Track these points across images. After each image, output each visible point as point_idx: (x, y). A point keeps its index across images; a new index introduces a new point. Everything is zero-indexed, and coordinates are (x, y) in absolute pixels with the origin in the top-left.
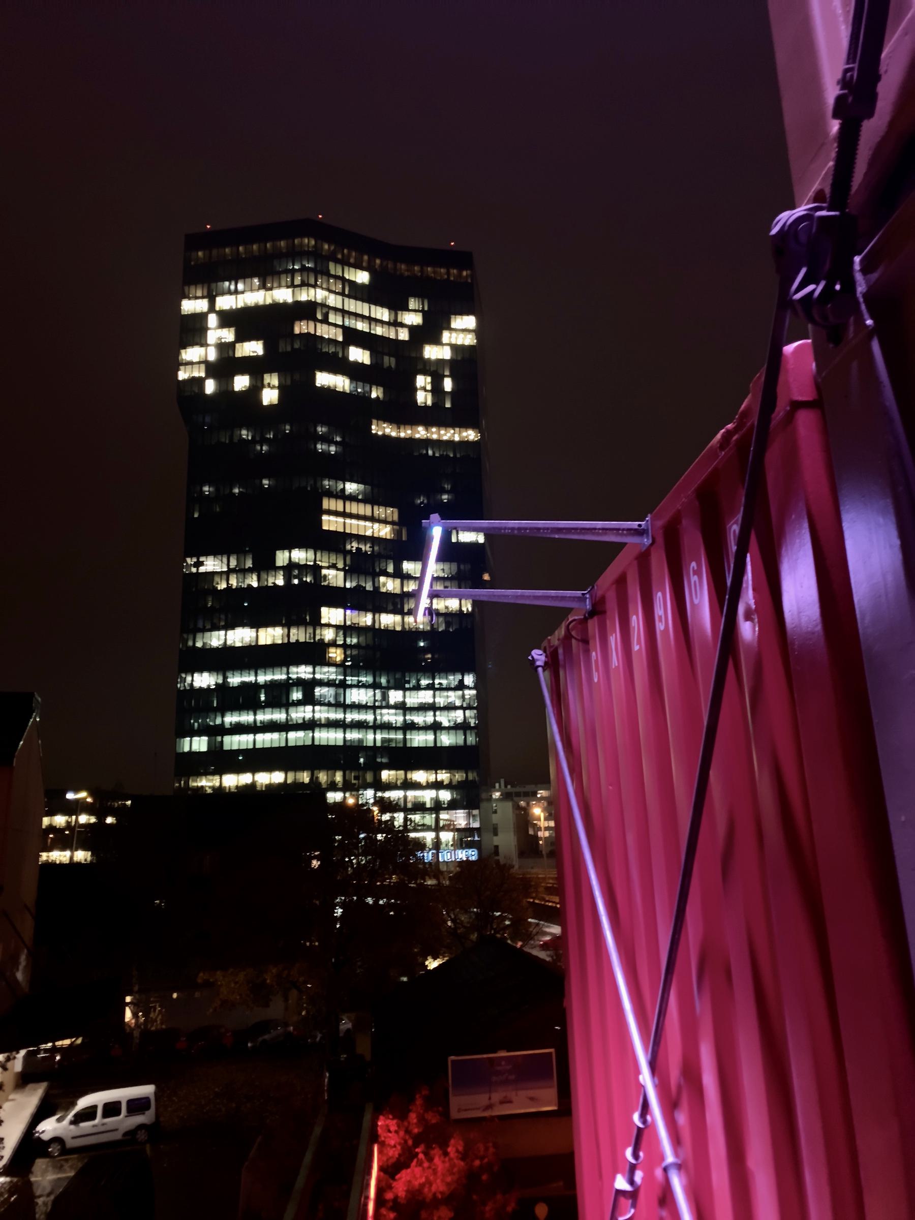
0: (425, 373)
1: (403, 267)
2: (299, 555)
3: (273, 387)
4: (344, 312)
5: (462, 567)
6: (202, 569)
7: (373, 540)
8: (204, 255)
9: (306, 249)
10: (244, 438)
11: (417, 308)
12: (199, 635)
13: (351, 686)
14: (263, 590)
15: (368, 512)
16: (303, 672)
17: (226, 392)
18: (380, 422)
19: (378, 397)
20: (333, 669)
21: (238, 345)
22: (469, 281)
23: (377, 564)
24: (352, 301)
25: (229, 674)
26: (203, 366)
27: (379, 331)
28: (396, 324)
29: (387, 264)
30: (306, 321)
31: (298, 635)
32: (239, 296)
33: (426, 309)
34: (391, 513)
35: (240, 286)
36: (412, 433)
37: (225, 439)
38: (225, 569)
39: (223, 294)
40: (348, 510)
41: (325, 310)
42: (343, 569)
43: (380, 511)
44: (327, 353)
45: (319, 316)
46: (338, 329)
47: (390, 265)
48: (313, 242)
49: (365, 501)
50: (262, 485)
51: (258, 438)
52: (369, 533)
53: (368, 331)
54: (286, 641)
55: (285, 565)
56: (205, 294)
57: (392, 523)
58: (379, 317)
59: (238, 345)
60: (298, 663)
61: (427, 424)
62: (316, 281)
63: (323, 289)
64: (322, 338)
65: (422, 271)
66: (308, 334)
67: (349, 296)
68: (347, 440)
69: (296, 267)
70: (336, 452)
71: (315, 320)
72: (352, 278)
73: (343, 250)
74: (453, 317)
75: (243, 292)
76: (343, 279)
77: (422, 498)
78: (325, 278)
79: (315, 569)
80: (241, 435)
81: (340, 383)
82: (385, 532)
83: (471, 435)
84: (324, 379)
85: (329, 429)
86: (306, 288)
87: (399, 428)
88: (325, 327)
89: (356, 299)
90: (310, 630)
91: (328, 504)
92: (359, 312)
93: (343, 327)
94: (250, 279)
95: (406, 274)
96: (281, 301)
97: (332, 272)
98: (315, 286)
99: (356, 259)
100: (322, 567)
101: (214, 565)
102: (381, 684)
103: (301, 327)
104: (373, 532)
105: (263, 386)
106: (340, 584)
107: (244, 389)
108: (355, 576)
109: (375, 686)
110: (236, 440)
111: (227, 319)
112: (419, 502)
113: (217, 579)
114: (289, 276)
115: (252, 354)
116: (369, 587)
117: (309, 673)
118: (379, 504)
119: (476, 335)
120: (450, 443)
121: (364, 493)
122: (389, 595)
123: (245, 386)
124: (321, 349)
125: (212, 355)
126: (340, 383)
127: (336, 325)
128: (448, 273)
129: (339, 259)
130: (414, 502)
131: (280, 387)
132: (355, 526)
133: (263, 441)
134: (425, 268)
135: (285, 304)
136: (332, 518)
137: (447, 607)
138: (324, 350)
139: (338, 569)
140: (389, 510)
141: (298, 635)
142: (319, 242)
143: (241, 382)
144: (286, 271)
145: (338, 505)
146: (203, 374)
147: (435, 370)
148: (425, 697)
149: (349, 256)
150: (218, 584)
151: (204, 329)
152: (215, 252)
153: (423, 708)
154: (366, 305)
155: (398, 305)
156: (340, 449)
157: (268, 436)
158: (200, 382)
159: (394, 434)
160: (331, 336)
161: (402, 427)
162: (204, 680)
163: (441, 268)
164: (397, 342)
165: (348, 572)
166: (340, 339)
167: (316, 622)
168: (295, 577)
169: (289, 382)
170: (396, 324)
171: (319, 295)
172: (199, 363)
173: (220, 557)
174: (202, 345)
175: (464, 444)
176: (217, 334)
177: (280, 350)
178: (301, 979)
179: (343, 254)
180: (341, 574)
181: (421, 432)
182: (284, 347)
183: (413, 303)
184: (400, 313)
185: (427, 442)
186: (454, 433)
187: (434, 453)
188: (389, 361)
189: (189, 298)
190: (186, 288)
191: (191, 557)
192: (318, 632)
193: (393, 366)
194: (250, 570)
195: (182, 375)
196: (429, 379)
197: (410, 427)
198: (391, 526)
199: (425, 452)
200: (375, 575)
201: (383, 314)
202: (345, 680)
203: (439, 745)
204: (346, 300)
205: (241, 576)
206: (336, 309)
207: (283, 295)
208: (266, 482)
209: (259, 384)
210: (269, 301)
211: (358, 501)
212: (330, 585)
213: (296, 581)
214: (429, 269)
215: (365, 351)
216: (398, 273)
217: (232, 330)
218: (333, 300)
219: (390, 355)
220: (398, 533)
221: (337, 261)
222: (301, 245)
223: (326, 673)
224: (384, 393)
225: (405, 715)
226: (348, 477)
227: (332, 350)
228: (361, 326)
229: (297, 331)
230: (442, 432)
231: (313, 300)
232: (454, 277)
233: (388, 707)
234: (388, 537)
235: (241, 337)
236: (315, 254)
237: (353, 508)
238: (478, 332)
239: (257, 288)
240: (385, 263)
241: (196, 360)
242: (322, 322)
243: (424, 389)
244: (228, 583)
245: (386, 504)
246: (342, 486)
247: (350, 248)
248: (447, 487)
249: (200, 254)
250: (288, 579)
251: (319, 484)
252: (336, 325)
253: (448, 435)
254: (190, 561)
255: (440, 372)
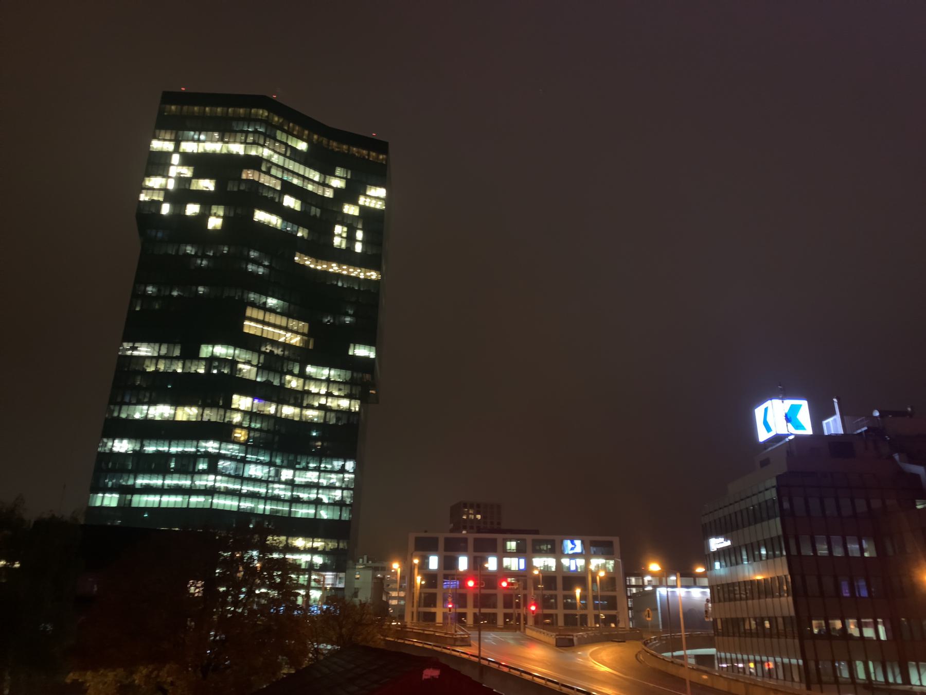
0: (342, 224)
1: (335, 144)
2: (220, 351)
3: (218, 217)
4: (284, 169)
5: (355, 375)
6: (136, 353)
7: (286, 346)
8: (176, 108)
9: (260, 118)
10: (188, 253)
11: (342, 176)
12: (124, 408)
13: (250, 462)
14: (186, 375)
15: (284, 324)
16: (211, 446)
17: (178, 216)
18: (302, 255)
19: (303, 236)
20: (236, 447)
21: (194, 181)
22: (384, 162)
23: (285, 365)
24: (292, 162)
25: (146, 442)
26: (162, 193)
27: (310, 187)
28: (324, 185)
29: (323, 139)
30: (252, 171)
31: (211, 415)
32: (201, 145)
33: (349, 177)
34: (303, 326)
35: (202, 137)
36: (327, 267)
37: (171, 251)
38: (156, 354)
39: (187, 140)
40: (267, 320)
41: (269, 165)
42: (257, 366)
43: (293, 324)
44: (266, 197)
45: (264, 169)
46: (278, 181)
47: (325, 141)
48: (266, 114)
49: (282, 314)
50: (197, 291)
51: (200, 254)
52: (282, 340)
53: (301, 186)
54: (199, 419)
55: (208, 357)
56: (173, 138)
57: (303, 334)
58: (311, 177)
59: (194, 181)
60: (207, 439)
61: (340, 262)
62: (265, 142)
63: (269, 149)
64: (263, 185)
65: (349, 150)
66: (253, 180)
67: (290, 158)
68: (273, 265)
69: (250, 130)
70: (263, 273)
71: (260, 170)
72: (294, 145)
73: (289, 124)
74: (368, 186)
75: (204, 142)
76: (286, 145)
77: (329, 318)
78: (272, 141)
79: (233, 363)
80: (185, 250)
81: (274, 221)
82: (296, 340)
83: (373, 275)
84: (260, 216)
85: (260, 254)
86: (256, 146)
87: (317, 262)
88: (267, 177)
89: (295, 160)
90: (222, 412)
91: (250, 312)
92: (296, 171)
93: (281, 179)
94: (211, 133)
95: (337, 149)
96: (235, 153)
97: (279, 138)
98: (263, 146)
99: (298, 132)
100: (238, 362)
101: (147, 352)
102: (276, 463)
103: (248, 174)
104: (285, 340)
105: (210, 215)
106: (252, 377)
107: (194, 215)
108: (265, 373)
109: (270, 464)
110: (181, 253)
111: (187, 159)
112: (326, 320)
113: (147, 362)
114: (244, 135)
115: (205, 189)
116: (276, 382)
117: (216, 448)
118: (294, 318)
119: (386, 203)
120: (357, 278)
121: (282, 308)
122: (292, 391)
123: (195, 213)
124: (262, 193)
125: (171, 185)
126: (274, 221)
127: (276, 178)
128: (369, 155)
129: (284, 129)
130: (322, 321)
131: (225, 218)
132: (270, 332)
133: (204, 256)
134: (351, 148)
135: (238, 155)
136: (253, 324)
137: (339, 406)
138: (264, 195)
139: (252, 365)
140: (301, 324)
141: (211, 415)
142: (271, 114)
143: (192, 209)
144: (242, 131)
145: (259, 315)
146: (161, 199)
147: (350, 223)
148: (312, 477)
149: (294, 129)
150: (147, 366)
151: (168, 164)
152: (185, 108)
153: (309, 486)
154: (302, 167)
155: (327, 171)
156: (267, 271)
157: (208, 254)
158: (158, 204)
159: (312, 266)
160: (271, 185)
161: (320, 261)
162: (122, 446)
163: (364, 149)
164: (323, 197)
165: (260, 368)
166: (279, 188)
167: (227, 406)
168: (215, 367)
169: (232, 214)
170: (324, 185)
171: (266, 153)
172: (160, 190)
173: (152, 344)
174: (164, 176)
175: (367, 281)
176: (177, 169)
177: (228, 189)
178: (170, 679)
179: (289, 127)
180: (255, 369)
181: (334, 268)
182: (232, 187)
183: (339, 171)
184: (328, 177)
185: (338, 276)
186: (361, 272)
187: (343, 285)
188: (315, 211)
189: (159, 140)
190: (157, 131)
191: (128, 341)
192: (228, 414)
193: (318, 215)
194: (177, 358)
195: (143, 197)
196: (345, 229)
197: (326, 262)
198: (302, 336)
199: (335, 283)
200: (283, 373)
201: (316, 176)
202: (245, 457)
203: (318, 517)
204: (287, 160)
205: (168, 362)
206: (277, 166)
207: (237, 148)
208: (201, 290)
209: (207, 213)
210: (224, 151)
211: (277, 313)
212: (244, 377)
213: (215, 371)
214: (355, 149)
215: (297, 201)
216: (330, 148)
217: (191, 168)
218: (276, 158)
219: (316, 206)
220: (306, 343)
221: (283, 131)
222: (257, 114)
223: (231, 449)
224: (309, 234)
225: (292, 491)
226: (270, 293)
227: (270, 195)
228: (295, 181)
229: (244, 176)
230: (351, 270)
231: (261, 156)
232: (373, 158)
233: (280, 482)
234: (298, 345)
235: (198, 175)
236: (266, 122)
237: (271, 318)
238: (387, 200)
239: (217, 140)
240: (321, 139)
241: (157, 187)
242: (265, 173)
243: (340, 235)
244: (156, 368)
245: (299, 318)
246: (264, 300)
247: (294, 123)
248: (351, 312)
249: (173, 108)
250: (208, 369)
251: (245, 297)
252: (276, 178)
253: (355, 272)
254: (127, 345)
255: (355, 225)
